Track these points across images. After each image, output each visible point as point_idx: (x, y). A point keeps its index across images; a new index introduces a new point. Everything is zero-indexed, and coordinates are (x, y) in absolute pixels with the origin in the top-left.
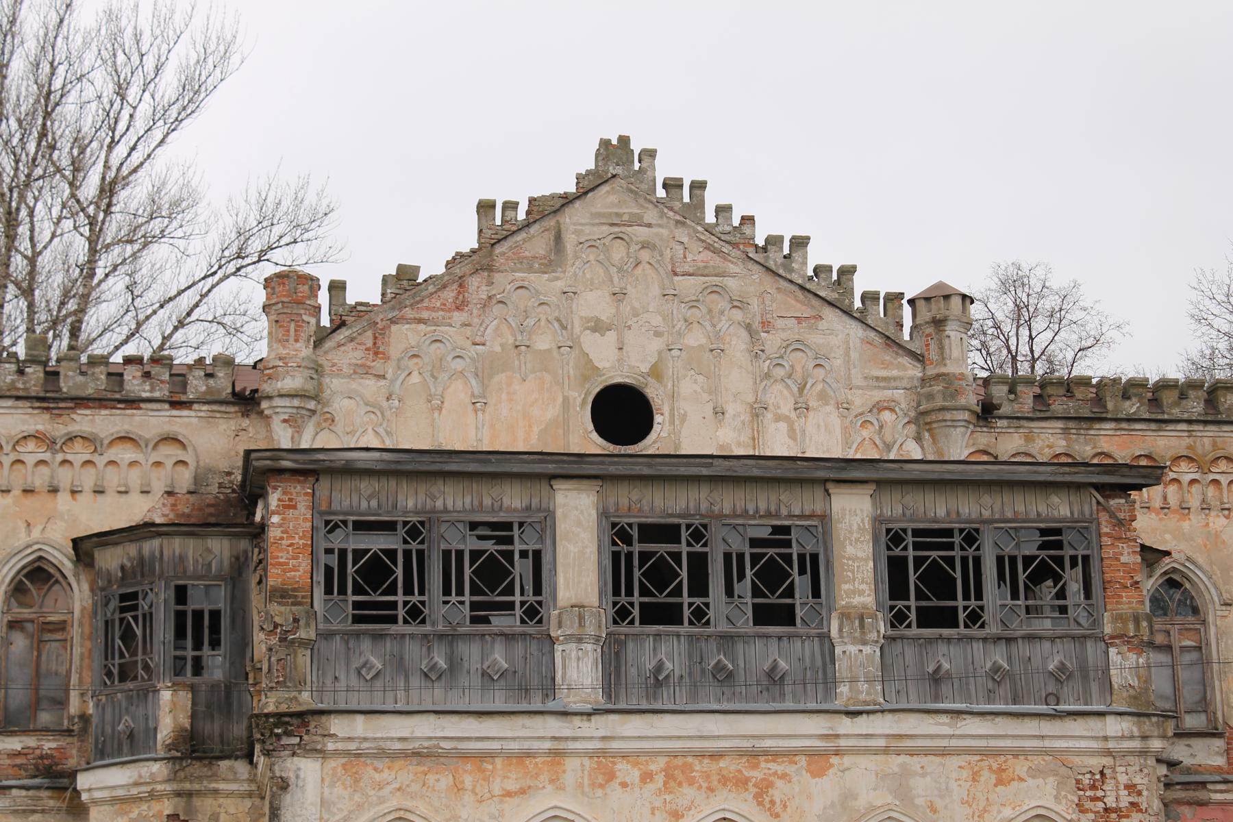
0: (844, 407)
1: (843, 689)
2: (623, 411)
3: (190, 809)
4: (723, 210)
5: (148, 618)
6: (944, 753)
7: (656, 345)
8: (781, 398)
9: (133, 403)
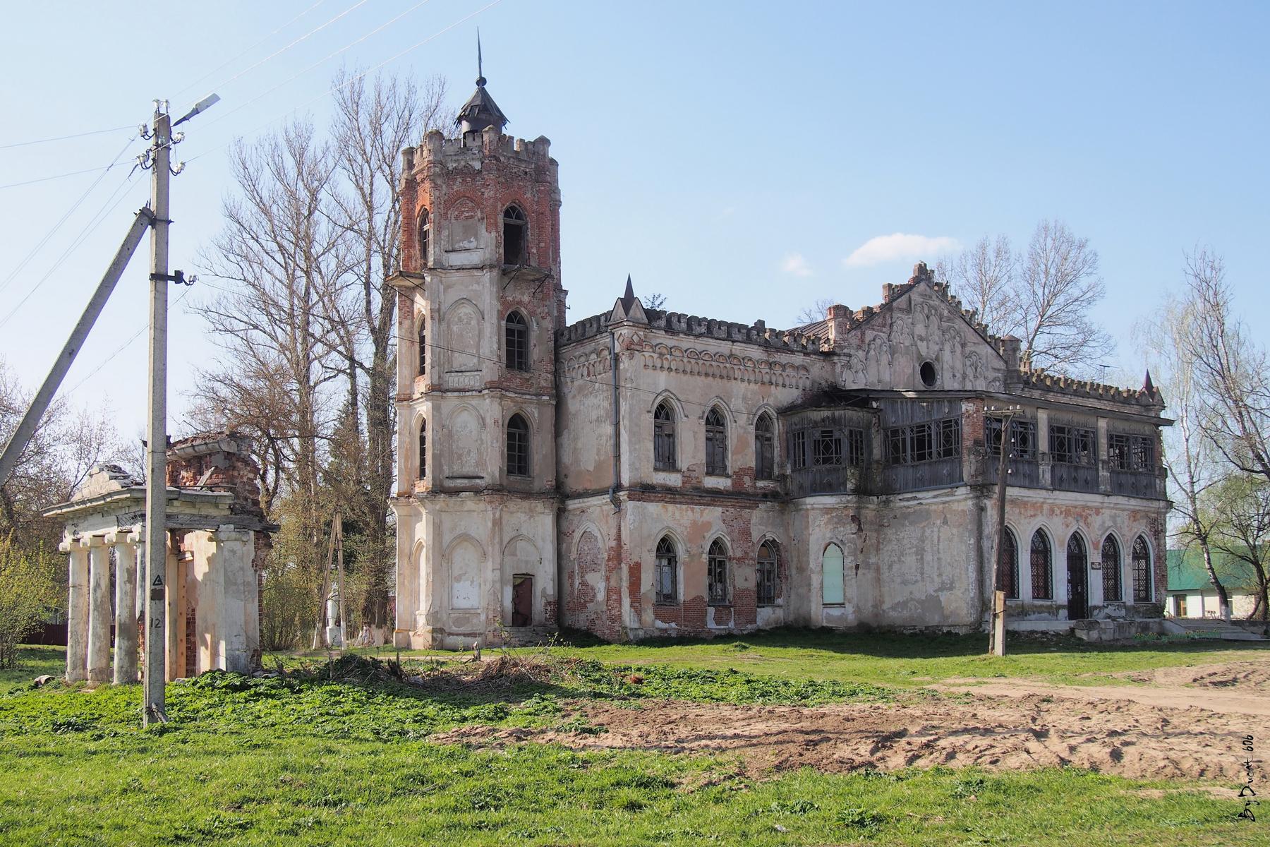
0: (985, 378)
1: (1102, 487)
2: (928, 372)
3: (859, 513)
4: (953, 297)
5: (838, 441)
6: (1123, 510)
7: (937, 348)
8: (970, 372)
9: (792, 352)
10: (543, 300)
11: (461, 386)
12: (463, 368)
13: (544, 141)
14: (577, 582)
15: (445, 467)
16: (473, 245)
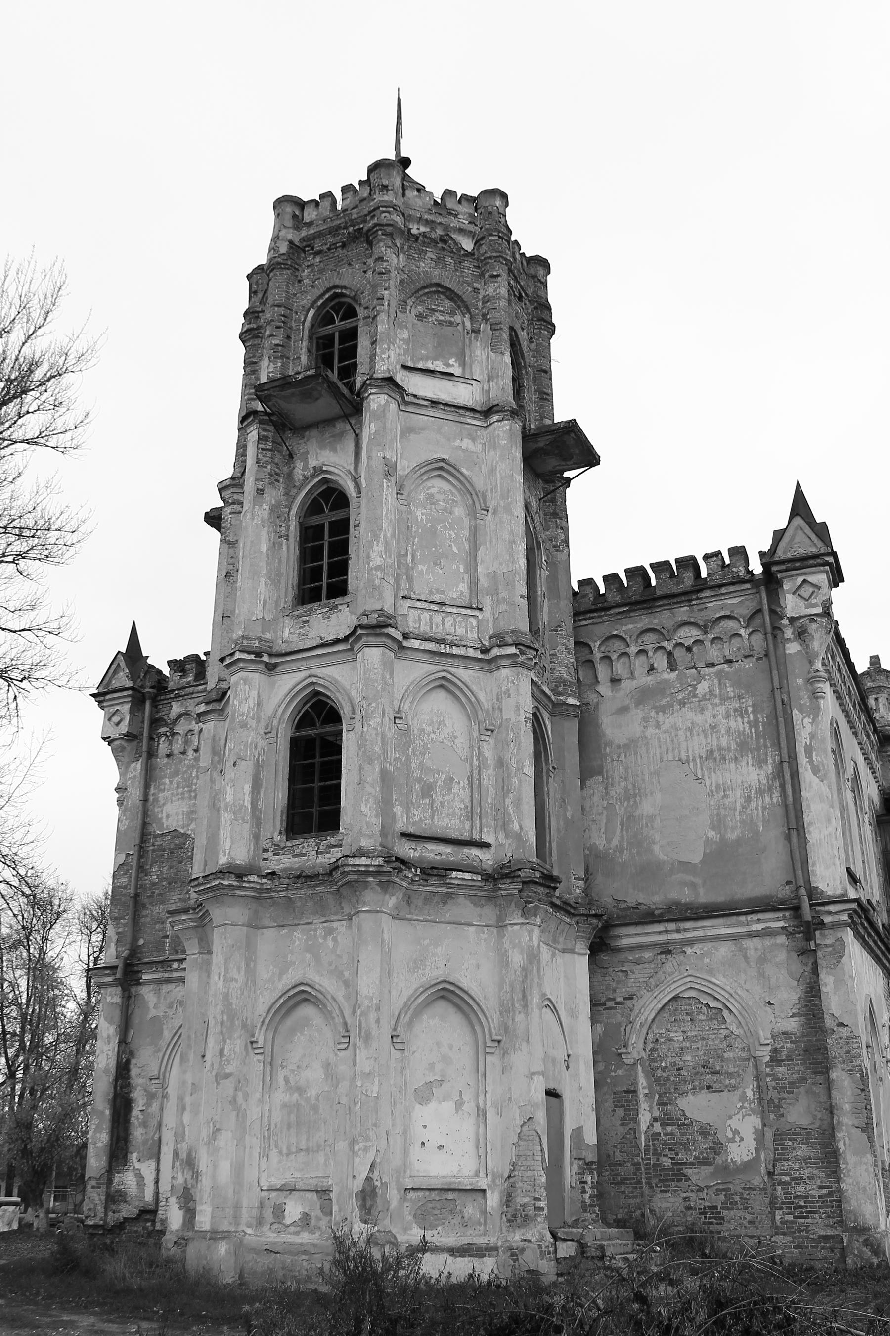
10: (555, 515)
11: (438, 631)
12: (436, 598)
13: (542, 263)
14: (644, 1119)
15: (398, 809)
16: (457, 370)
